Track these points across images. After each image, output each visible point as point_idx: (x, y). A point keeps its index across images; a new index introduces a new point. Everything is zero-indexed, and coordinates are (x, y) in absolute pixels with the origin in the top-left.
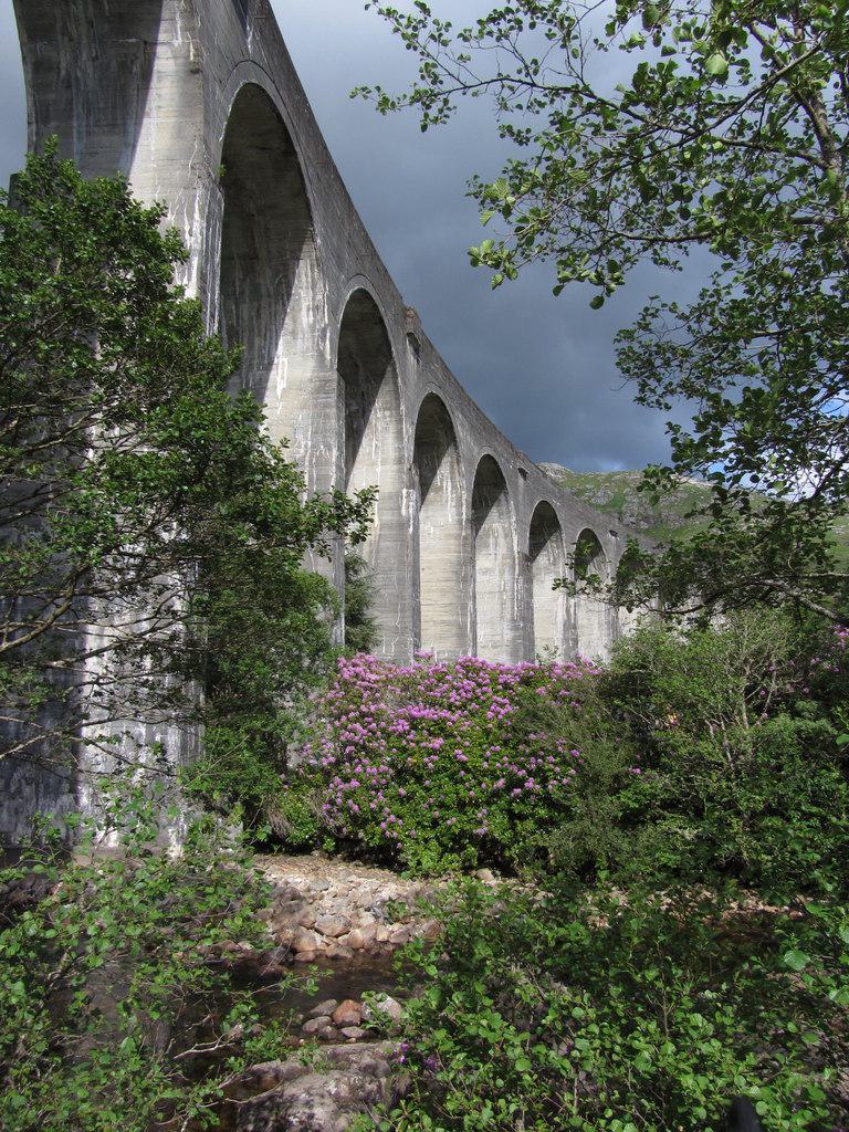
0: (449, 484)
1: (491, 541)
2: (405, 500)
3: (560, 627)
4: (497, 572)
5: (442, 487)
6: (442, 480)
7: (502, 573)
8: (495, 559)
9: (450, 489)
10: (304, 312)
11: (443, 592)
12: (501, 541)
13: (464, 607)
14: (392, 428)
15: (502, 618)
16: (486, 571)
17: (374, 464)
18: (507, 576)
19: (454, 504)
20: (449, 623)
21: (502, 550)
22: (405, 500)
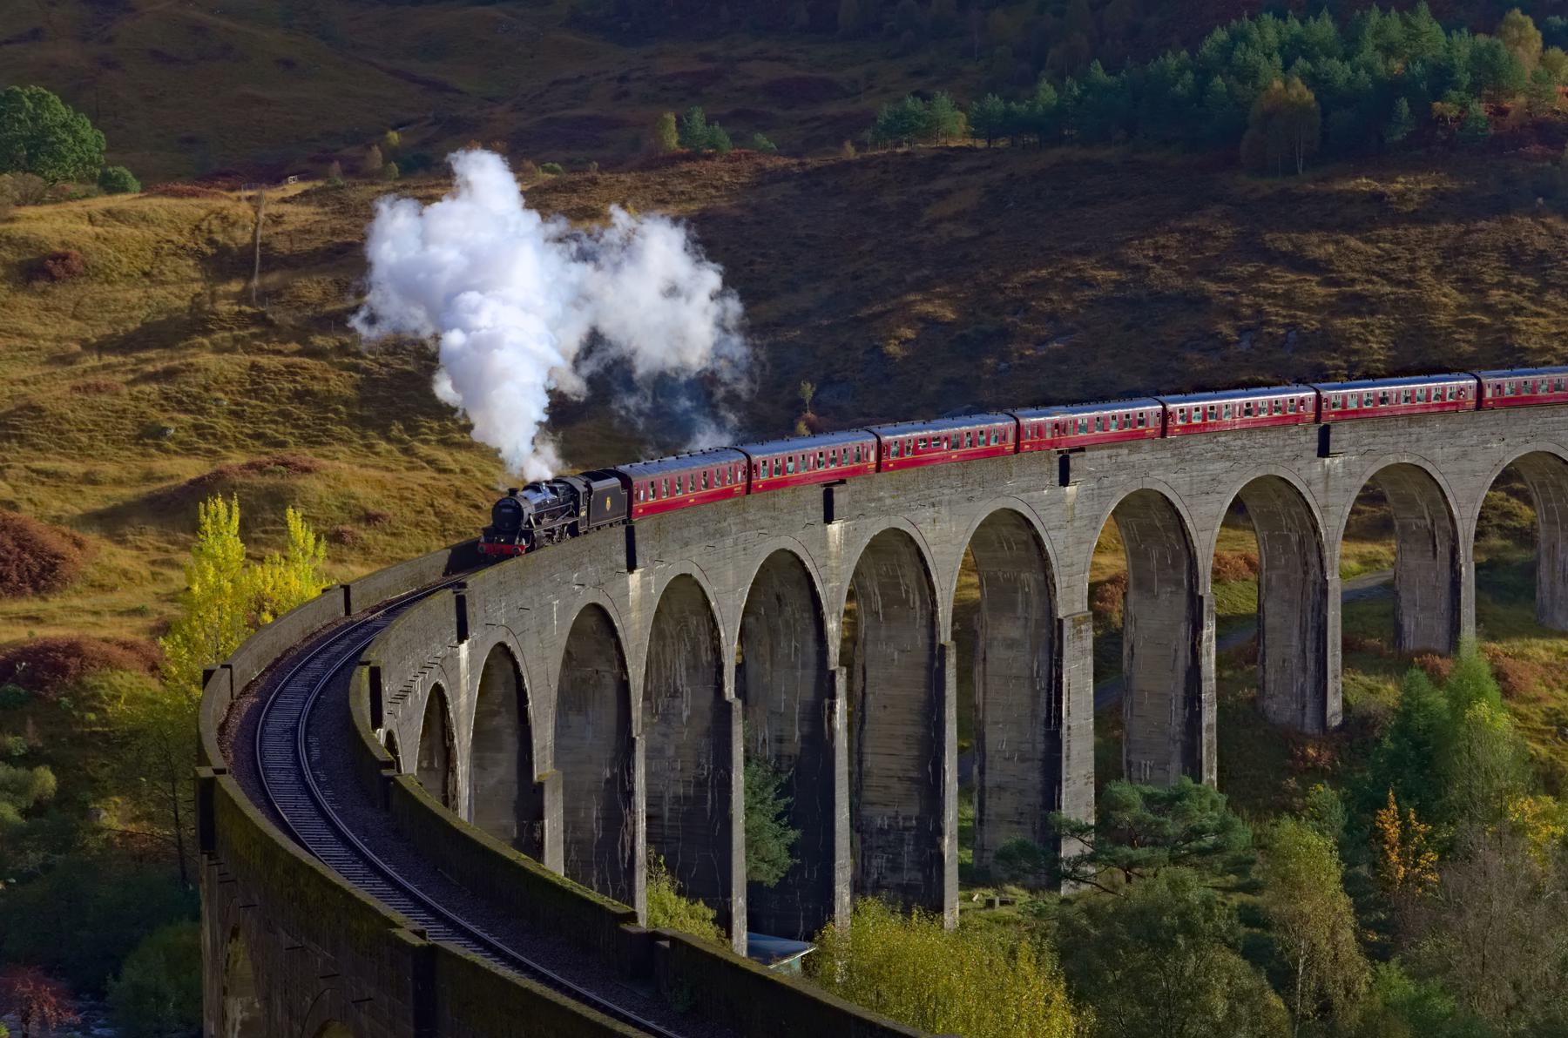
0: (917, 597)
1: (1020, 597)
2: (827, 712)
3: (1181, 676)
4: (1028, 646)
5: (907, 600)
6: (907, 592)
8: (1026, 626)
9: (918, 603)
10: (703, 652)
15: (1034, 716)
16: (1011, 644)
17: (794, 667)
19: (924, 622)
21: (1036, 613)
22: (827, 712)
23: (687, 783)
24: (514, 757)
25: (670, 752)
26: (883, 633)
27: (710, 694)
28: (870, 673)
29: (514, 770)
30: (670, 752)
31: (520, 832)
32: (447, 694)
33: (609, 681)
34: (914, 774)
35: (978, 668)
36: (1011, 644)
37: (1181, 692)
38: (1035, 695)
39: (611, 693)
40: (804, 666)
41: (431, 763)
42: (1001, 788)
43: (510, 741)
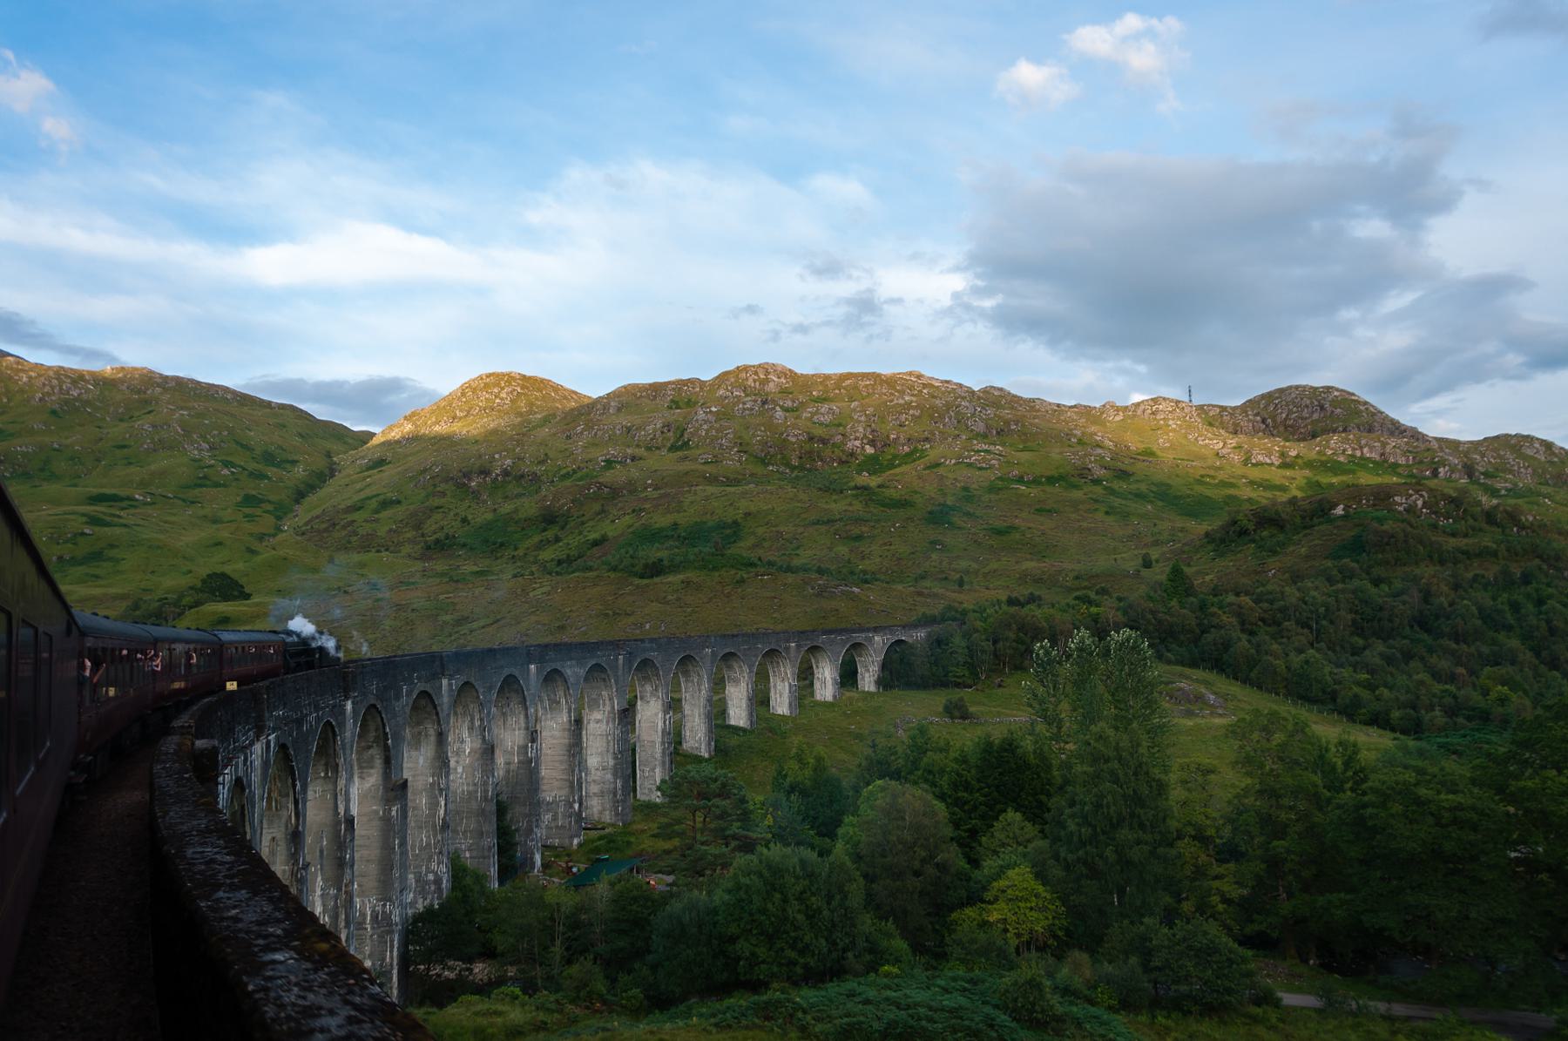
3: (660, 734)
7: (608, 723)
11: (561, 762)
12: (607, 702)
13: (573, 771)
14: (523, 713)
16: (598, 721)
17: (514, 730)
18: (611, 725)
20: (566, 780)
21: (608, 708)
23: (468, 784)
24: (381, 771)
25: (460, 770)
26: (549, 716)
27: (480, 741)
28: (543, 734)
29: (380, 778)
30: (460, 770)
31: (384, 813)
32: (337, 730)
33: (432, 732)
34: (565, 777)
35: (584, 732)
36: (598, 721)
37: (660, 740)
38: (608, 742)
39: (433, 739)
40: (519, 729)
41: (327, 774)
42: (594, 781)
43: (378, 762)
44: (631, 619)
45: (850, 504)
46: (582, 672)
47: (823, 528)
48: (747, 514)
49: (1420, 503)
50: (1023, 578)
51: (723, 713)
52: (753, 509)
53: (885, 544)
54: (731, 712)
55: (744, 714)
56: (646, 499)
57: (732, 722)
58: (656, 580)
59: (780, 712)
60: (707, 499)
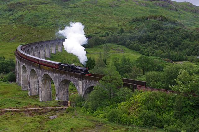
44: (33, 34)
45: (69, 11)
46: (35, 47)
47: (64, 16)
48: (50, 12)
49: (161, 19)
50: (99, 27)
51: (51, 51)
52: (51, 11)
53: (75, 19)
54: (52, 51)
55: (54, 52)
56: (29, 7)
57: (53, 53)
58: (36, 27)
59: (59, 51)
60: (42, 8)
